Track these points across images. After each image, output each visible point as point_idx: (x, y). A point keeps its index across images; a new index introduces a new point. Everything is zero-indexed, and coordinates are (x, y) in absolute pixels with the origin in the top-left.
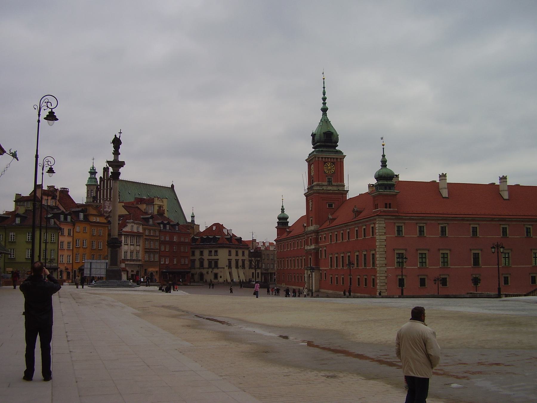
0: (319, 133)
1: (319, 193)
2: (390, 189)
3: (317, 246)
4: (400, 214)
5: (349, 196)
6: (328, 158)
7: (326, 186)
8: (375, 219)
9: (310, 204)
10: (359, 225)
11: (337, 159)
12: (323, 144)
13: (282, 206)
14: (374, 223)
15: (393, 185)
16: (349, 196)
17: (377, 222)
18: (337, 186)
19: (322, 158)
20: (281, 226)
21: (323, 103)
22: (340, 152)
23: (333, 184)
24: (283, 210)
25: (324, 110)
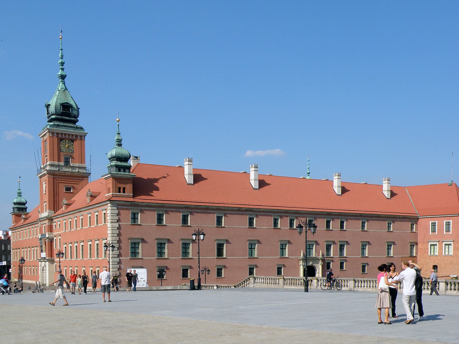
1: (53, 175)
2: (124, 171)
3: (51, 236)
4: (136, 200)
6: (65, 134)
8: (107, 204)
11: (76, 136)
15: (129, 168)
22: (82, 128)
23: (71, 165)
24: (20, 194)
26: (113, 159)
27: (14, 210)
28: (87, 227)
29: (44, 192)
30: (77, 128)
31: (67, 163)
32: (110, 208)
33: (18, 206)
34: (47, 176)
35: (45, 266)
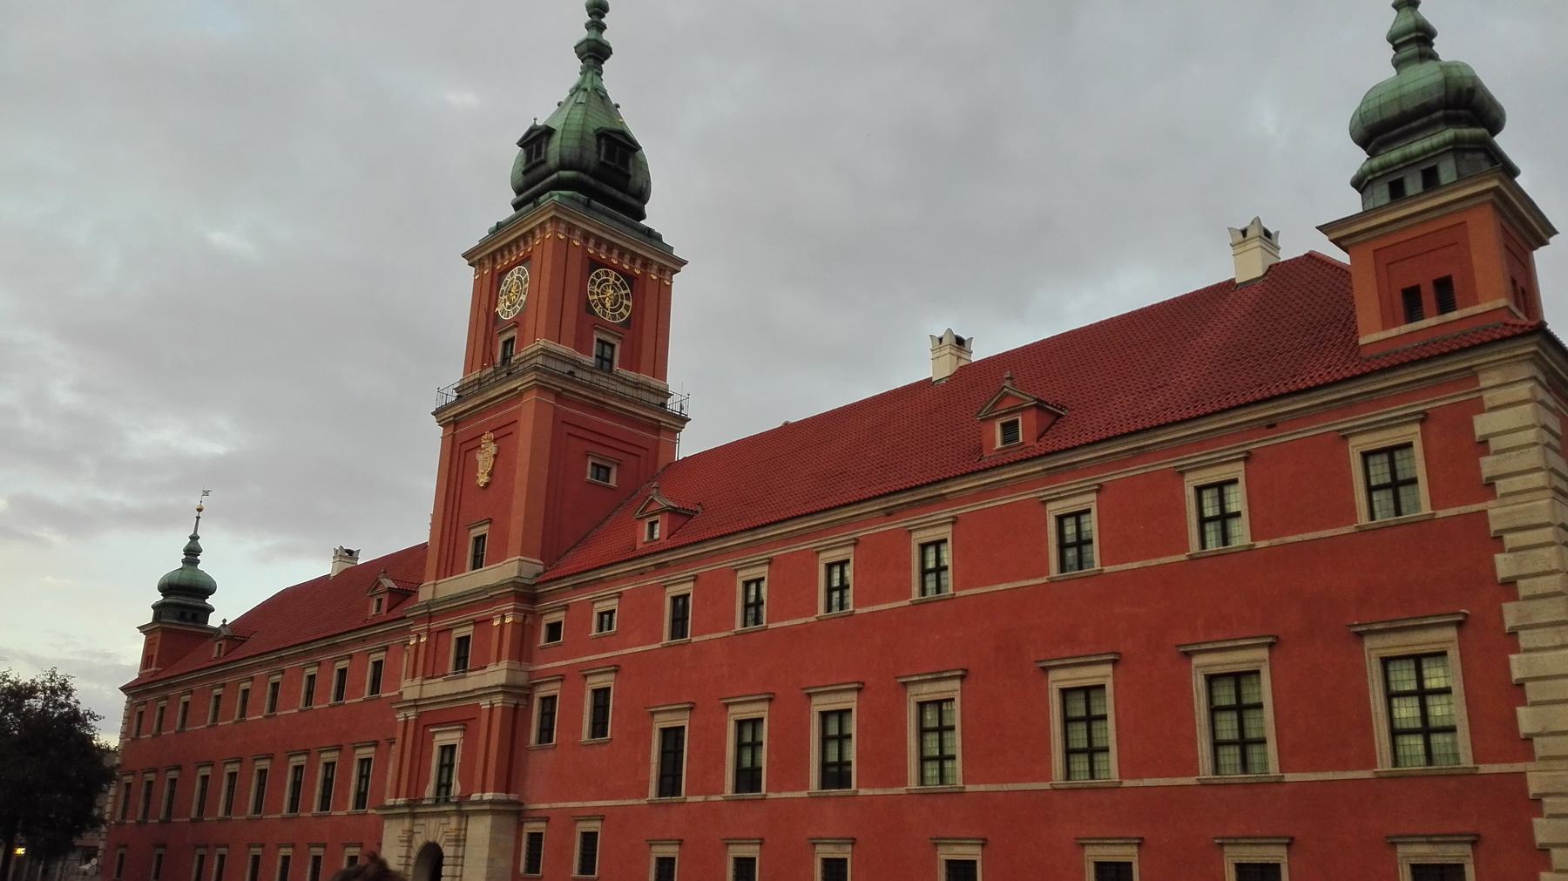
0: (573, 128)
1: (558, 396)
3: (521, 679)
5: (688, 445)
6: (611, 247)
7: (590, 370)
8: (1471, 375)
9: (485, 459)
10: (1107, 478)
11: (646, 263)
12: (592, 181)
13: (194, 538)
14: (1424, 419)
16: (688, 445)
17: (1490, 398)
18: (637, 386)
19: (586, 236)
20: (172, 622)
21: (588, 27)
24: (192, 553)
25: (595, 53)
26: (1379, 138)
27: (157, 617)
28: (1041, 576)
29: (483, 479)
30: (650, 234)
31: (605, 362)
32: (1532, 390)
33: (181, 600)
34: (531, 397)
35: (460, 840)
